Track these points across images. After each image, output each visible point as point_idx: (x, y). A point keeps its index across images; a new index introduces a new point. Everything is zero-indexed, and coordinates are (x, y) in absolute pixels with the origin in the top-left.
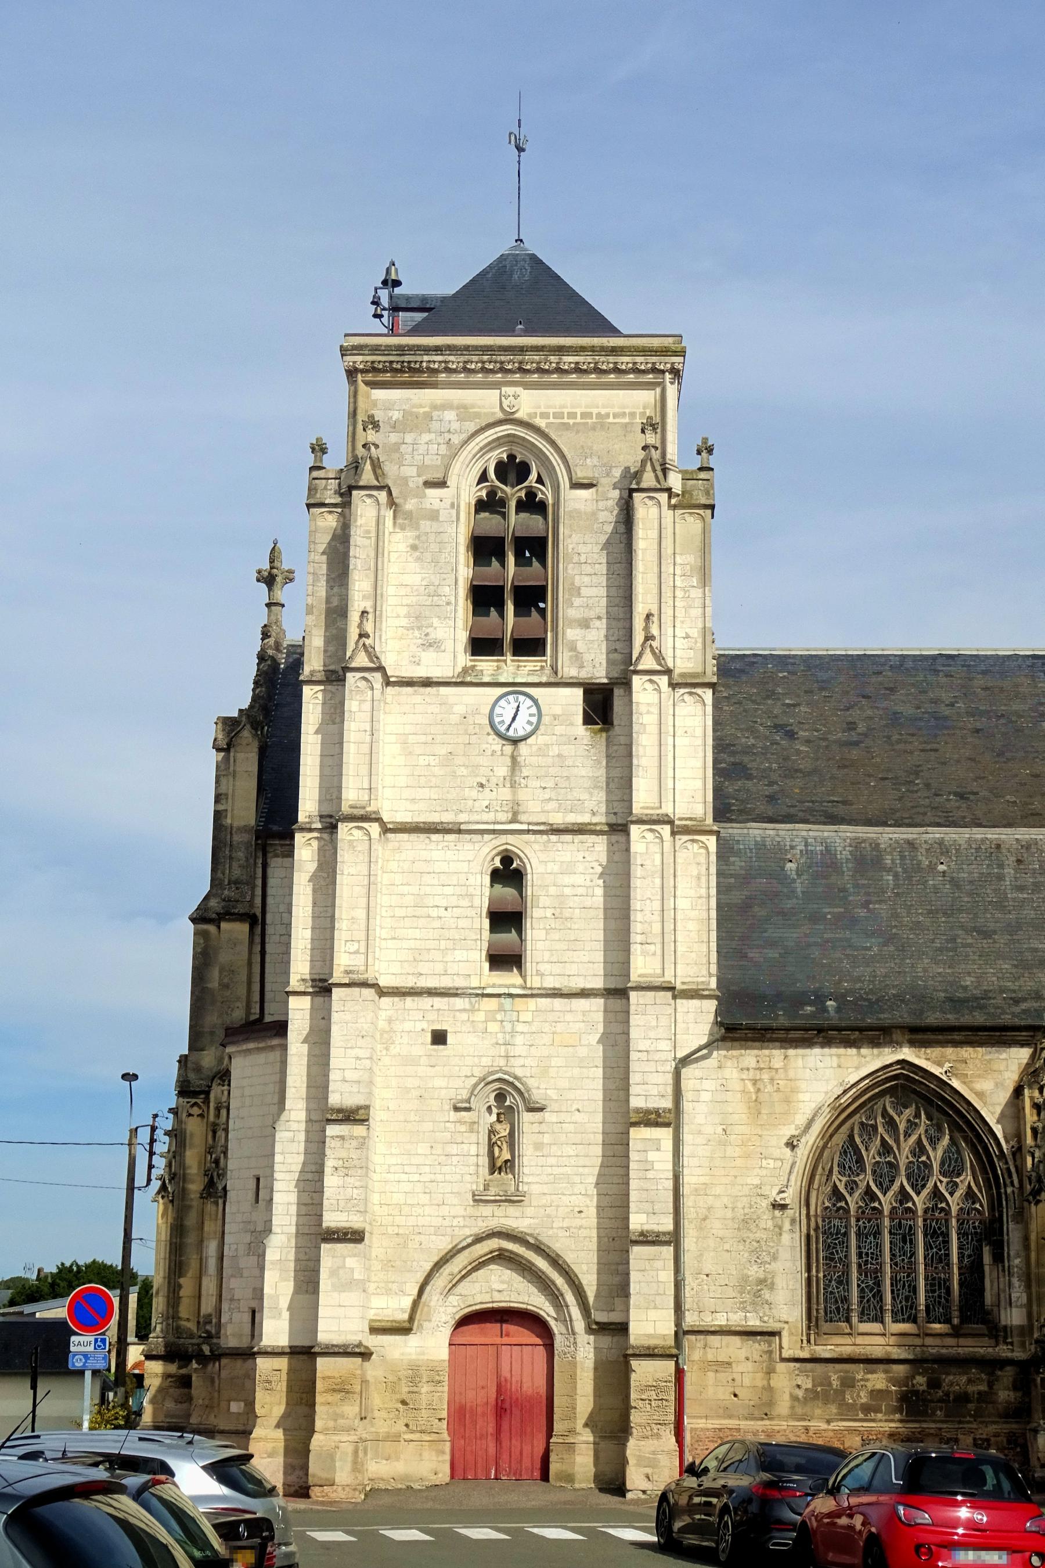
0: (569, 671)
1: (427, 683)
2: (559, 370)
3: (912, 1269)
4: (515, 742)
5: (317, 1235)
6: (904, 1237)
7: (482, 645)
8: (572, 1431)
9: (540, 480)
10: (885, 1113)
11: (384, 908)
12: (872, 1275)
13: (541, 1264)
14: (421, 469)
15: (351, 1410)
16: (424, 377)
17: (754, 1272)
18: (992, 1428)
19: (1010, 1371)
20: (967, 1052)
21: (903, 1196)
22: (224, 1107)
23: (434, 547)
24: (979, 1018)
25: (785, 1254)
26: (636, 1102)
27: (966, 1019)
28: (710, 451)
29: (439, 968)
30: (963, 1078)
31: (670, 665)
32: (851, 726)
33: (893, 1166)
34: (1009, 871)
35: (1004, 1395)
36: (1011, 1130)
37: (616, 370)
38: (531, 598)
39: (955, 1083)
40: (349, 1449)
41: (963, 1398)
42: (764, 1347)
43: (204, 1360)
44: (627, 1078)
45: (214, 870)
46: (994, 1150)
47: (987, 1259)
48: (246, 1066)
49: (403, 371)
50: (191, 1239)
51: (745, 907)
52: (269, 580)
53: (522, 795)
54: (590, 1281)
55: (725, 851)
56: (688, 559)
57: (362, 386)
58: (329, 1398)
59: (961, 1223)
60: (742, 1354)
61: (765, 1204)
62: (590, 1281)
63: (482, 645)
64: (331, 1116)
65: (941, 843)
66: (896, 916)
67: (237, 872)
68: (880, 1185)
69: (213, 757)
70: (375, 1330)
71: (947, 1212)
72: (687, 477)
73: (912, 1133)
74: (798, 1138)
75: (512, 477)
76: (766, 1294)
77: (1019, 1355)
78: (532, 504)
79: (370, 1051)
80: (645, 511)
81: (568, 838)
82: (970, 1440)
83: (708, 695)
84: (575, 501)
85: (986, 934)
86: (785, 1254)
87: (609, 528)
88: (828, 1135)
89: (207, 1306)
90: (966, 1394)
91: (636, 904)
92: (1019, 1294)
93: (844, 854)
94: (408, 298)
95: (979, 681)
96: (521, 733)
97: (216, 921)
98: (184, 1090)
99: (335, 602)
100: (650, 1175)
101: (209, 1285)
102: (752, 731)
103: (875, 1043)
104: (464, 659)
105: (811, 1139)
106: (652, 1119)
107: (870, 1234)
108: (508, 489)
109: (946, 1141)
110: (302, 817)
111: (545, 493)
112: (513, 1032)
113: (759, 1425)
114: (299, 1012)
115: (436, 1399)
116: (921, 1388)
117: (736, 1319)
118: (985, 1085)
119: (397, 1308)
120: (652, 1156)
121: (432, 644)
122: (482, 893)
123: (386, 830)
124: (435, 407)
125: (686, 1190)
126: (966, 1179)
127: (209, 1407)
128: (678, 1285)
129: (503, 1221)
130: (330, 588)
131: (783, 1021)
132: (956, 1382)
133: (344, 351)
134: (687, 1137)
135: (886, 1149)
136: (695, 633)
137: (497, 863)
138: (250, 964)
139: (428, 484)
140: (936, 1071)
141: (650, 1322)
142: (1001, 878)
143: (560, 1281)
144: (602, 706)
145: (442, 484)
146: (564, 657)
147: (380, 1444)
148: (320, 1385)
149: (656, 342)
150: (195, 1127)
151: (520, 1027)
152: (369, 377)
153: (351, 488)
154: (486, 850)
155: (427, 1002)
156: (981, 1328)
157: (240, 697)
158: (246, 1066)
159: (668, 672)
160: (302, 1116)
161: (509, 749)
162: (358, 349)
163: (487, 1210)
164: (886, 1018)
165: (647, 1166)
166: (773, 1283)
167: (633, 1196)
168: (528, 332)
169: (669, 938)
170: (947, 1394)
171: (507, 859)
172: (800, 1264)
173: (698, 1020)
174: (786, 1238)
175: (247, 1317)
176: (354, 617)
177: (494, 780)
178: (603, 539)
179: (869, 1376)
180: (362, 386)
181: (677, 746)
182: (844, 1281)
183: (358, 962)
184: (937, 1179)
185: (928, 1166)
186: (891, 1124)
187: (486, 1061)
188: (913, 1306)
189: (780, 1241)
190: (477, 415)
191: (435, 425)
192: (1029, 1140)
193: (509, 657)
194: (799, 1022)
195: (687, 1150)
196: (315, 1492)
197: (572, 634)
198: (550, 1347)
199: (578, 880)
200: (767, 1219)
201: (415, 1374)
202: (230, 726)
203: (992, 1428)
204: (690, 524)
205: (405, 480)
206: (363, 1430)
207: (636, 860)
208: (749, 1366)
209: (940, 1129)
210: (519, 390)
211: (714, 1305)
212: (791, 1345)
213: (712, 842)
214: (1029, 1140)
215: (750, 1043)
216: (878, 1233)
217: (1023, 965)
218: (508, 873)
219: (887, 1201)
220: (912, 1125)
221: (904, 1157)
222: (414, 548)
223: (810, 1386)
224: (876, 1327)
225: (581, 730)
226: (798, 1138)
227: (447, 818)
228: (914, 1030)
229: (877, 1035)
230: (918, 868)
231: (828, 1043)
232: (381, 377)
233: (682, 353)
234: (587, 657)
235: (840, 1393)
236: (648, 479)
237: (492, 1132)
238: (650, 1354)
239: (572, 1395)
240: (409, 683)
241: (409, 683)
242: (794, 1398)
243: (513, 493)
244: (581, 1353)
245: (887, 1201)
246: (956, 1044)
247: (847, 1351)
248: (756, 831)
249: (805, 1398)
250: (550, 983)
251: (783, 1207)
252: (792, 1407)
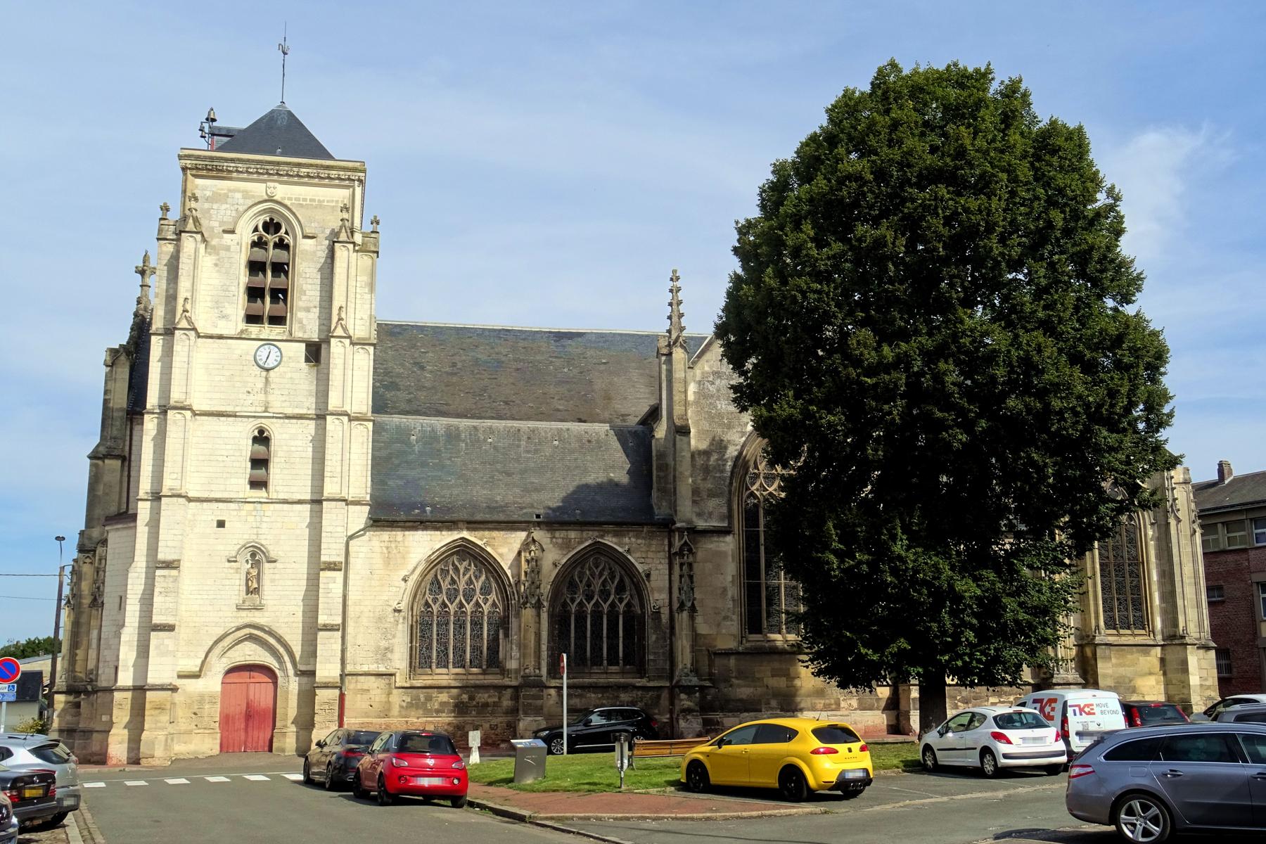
0: (298, 334)
1: (221, 337)
2: (298, 176)
3: (464, 639)
4: (268, 370)
5: (149, 627)
6: (460, 626)
7: (252, 319)
8: (285, 726)
9: (286, 233)
10: (453, 564)
11: (191, 456)
12: (444, 645)
13: (272, 641)
14: (222, 223)
15: (165, 718)
16: (225, 174)
17: (383, 644)
18: (500, 719)
19: (509, 691)
20: (495, 534)
21: (461, 605)
22: (103, 559)
23: (227, 265)
24: (502, 517)
25: (399, 635)
26: (323, 558)
27: (495, 517)
28: (378, 223)
29: (222, 487)
30: (493, 546)
31: (351, 333)
32: (454, 365)
33: (457, 591)
34: (523, 443)
35: (507, 703)
36: (515, 572)
37: (329, 178)
38: (280, 294)
39: (489, 549)
40: (163, 738)
41: (486, 705)
43: (87, 693)
44: (320, 546)
45: (102, 431)
46: (506, 582)
47: (501, 636)
48: (115, 536)
49: (211, 170)
50: (83, 629)
51: (388, 458)
52: (142, 273)
53: (271, 398)
54: (297, 650)
55: (378, 430)
56: (364, 279)
57: (190, 177)
58: (153, 712)
59: (489, 618)
60: (376, 685)
61: (390, 609)
62: (297, 650)
63: (252, 319)
64: (157, 565)
65: (490, 428)
66: (465, 464)
67: (115, 433)
68: (449, 600)
69: (104, 370)
70: (180, 677)
71: (482, 613)
72: (365, 235)
73: (466, 574)
74: (408, 576)
75: (272, 230)
76: (389, 655)
77: (514, 683)
78: (281, 245)
79: (182, 531)
80: (341, 253)
82: (487, 726)
83: (371, 349)
84: (304, 245)
85: (509, 474)
86: (399, 635)
87: (323, 260)
88: (424, 575)
89: (91, 665)
91: (327, 457)
92: (515, 653)
93: (441, 432)
94: (220, 129)
95: (521, 344)
96: (271, 366)
97: (103, 458)
98: (82, 549)
99: (171, 291)
101: (92, 654)
102: (402, 365)
103: (449, 529)
104: (242, 325)
105: (415, 576)
106: (332, 567)
107: (443, 624)
108: (269, 237)
109: (483, 577)
110: (148, 406)
111: (289, 240)
112: (261, 521)
113: (383, 720)
114: (144, 510)
115: (214, 712)
117: (373, 668)
118: (504, 550)
119: (193, 665)
120: (331, 586)
121: (224, 317)
122: (247, 449)
123: (195, 414)
124: (230, 191)
125: (350, 603)
126: (493, 597)
127: (91, 719)
128: (343, 651)
130: (168, 284)
131: (403, 517)
132: (483, 697)
133: (180, 157)
134: (351, 576)
135: (453, 582)
136: (366, 317)
137: (256, 433)
138: (121, 482)
139: (225, 232)
140: (479, 543)
141: (327, 670)
142: (519, 446)
143: (281, 650)
144: (315, 353)
145: (233, 232)
146: (296, 327)
147: (183, 734)
148: (147, 706)
149: (350, 165)
150: (87, 569)
151: (265, 519)
152: (194, 172)
153: (181, 232)
154: (250, 426)
155: (215, 505)
156: (497, 670)
157: (122, 337)
158: (115, 536)
159: (350, 337)
160: (144, 564)
161: (264, 373)
162: (188, 157)
163: (244, 614)
164: (455, 516)
165: (329, 591)
167: (320, 606)
168: (282, 155)
169: (345, 474)
171: (261, 431)
172: (407, 639)
173: (360, 516)
174: (400, 626)
175: (113, 671)
176: (180, 301)
178: (319, 266)
180: (190, 177)
181: (353, 375)
182: (429, 648)
183: (176, 484)
184: (478, 597)
185: (474, 590)
186: (456, 569)
187: (246, 537)
188: (464, 660)
190: (253, 197)
191: (229, 200)
192: (523, 578)
193: (266, 325)
194: (411, 518)
195: (351, 582)
196: (143, 762)
197: (300, 315)
198: (275, 683)
199: (299, 443)
200: (391, 617)
201: (201, 699)
202: (114, 353)
203: (500, 719)
204: (365, 260)
205: (213, 228)
206: (171, 729)
207: (329, 434)
208: (379, 691)
209: (481, 572)
210: (277, 185)
211: (361, 661)
212: (400, 680)
213: (370, 425)
214: (523, 578)
216: (447, 624)
217: (526, 490)
218: (262, 438)
219: (452, 608)
220: (467, 570)
221: (462, 585)
222: (216, 265)
224: (444, 671)
225: (303, 365)
226: (408, 576)
227: (229, 409)
228: (469, 522)
229: (451, 525)
230: (478, 441)
231: (426, 529)
232: (200, 173)
233: (364, 171)
234: (308, 327)
235: (425, 704)
236: (343, 237)
237: (248, 573)
238: (326, 686)
239: (286, 708)
240: (211, 337)
241: (211, 337)
242: (401, 707)
243: (271, 239)
244: (291, 685)
245: (452, 608)
246: (489, 529)
247: (429, 683)
248: (396, 419)
250: (282, 496)
251: (400, 611)
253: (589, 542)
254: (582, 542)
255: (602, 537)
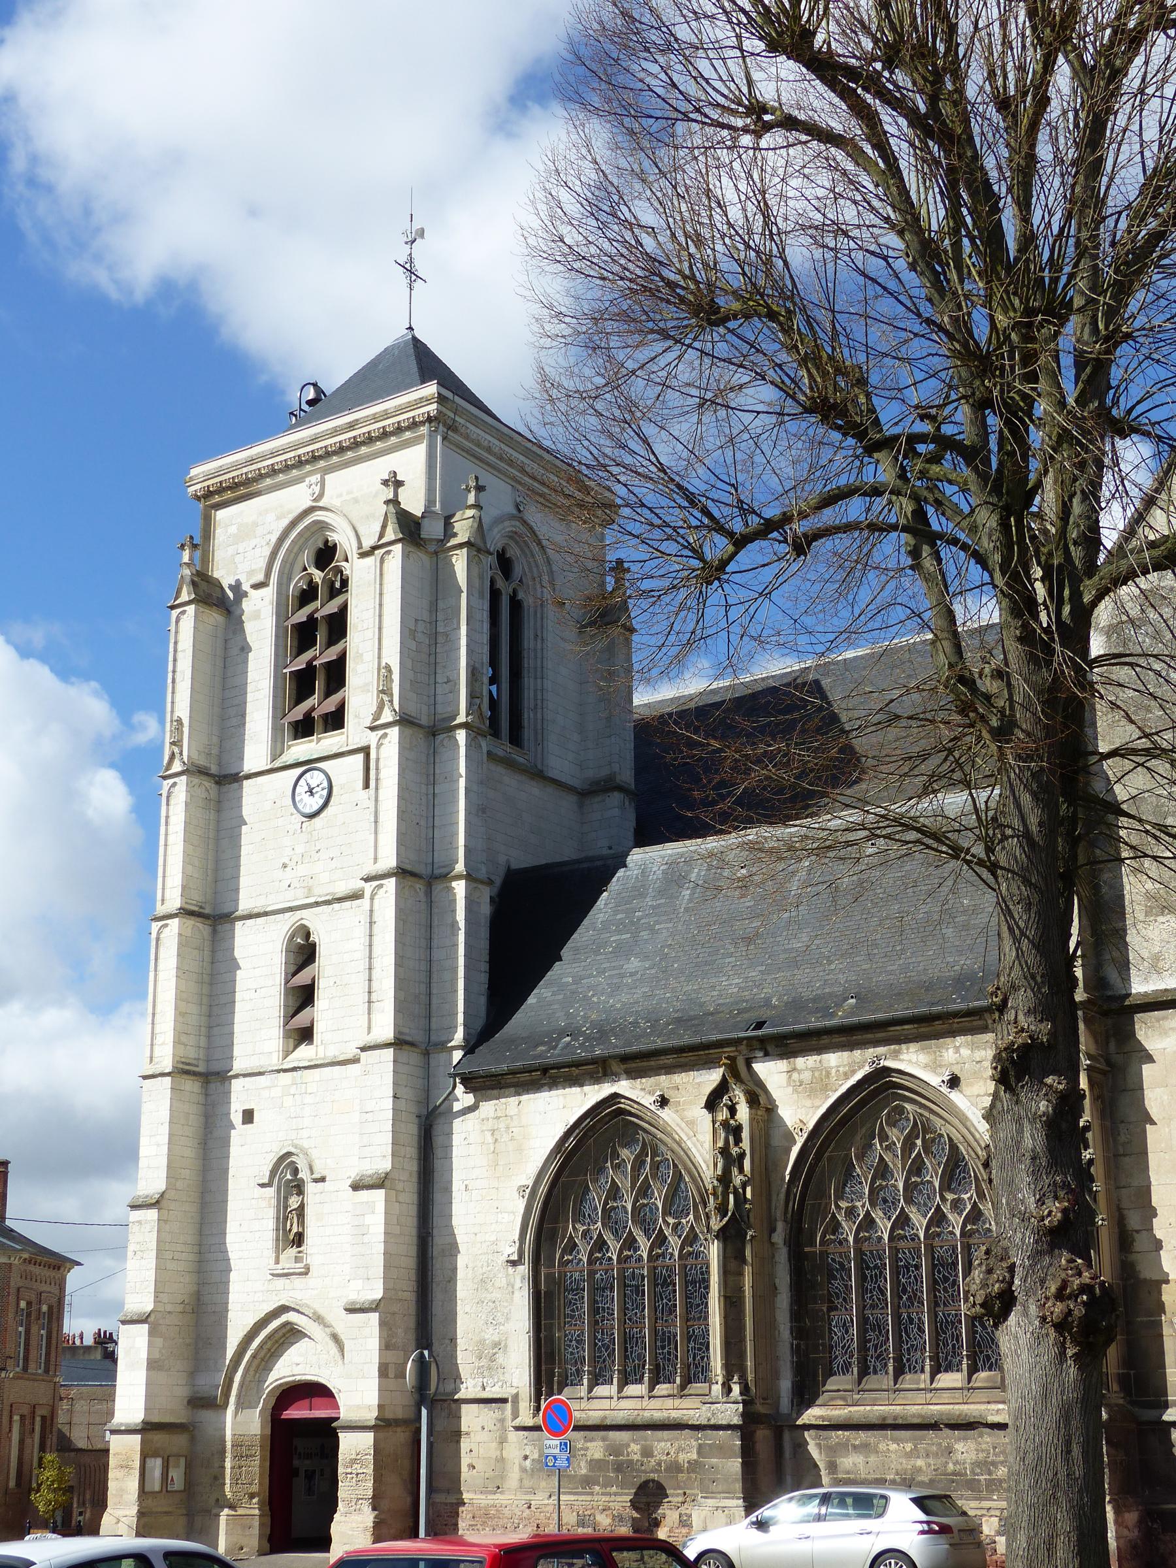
42: (498, 1414)
81: (347, 904)
90: (676, 1462)
100: (366, 1239)
116: (635, 1457)
129: (291, 1294)
151: (308, 1099)
166: (506, 1346)
170: (659, 1464)
174: (517, 1294)
177: (295, 859)
179: (589, 1444)
189: (512, 1299)
215: (489, 1092)
223: (536, 1456)
228: (625, 1059)
231: (554, 1084)
242: (523, 1470)
249: (532, 1470)
252: (521, 1480)
253: (867, 1069)
254: (854, 1072)
255: (896, 1055)
